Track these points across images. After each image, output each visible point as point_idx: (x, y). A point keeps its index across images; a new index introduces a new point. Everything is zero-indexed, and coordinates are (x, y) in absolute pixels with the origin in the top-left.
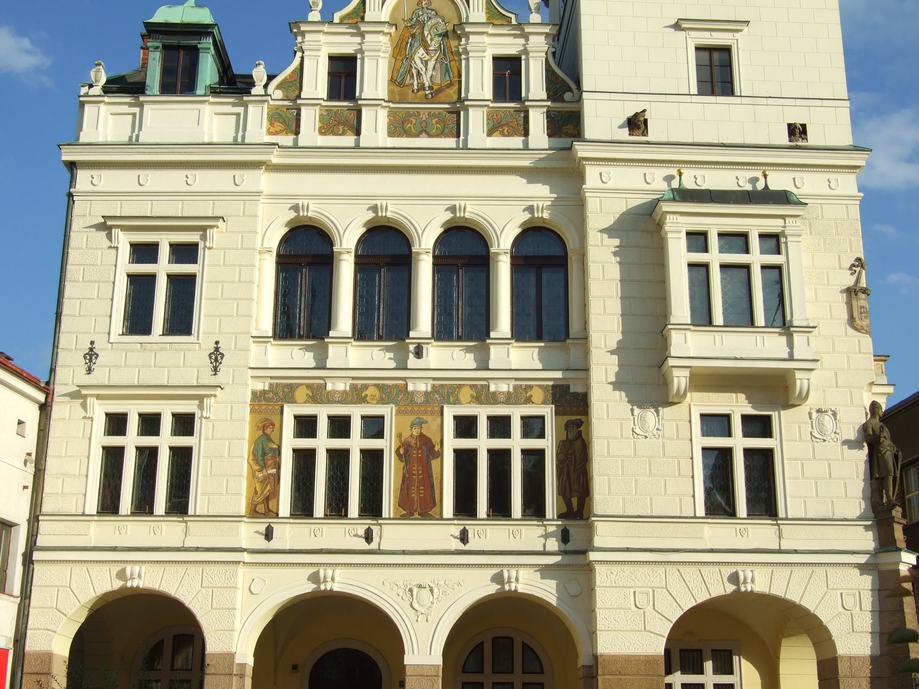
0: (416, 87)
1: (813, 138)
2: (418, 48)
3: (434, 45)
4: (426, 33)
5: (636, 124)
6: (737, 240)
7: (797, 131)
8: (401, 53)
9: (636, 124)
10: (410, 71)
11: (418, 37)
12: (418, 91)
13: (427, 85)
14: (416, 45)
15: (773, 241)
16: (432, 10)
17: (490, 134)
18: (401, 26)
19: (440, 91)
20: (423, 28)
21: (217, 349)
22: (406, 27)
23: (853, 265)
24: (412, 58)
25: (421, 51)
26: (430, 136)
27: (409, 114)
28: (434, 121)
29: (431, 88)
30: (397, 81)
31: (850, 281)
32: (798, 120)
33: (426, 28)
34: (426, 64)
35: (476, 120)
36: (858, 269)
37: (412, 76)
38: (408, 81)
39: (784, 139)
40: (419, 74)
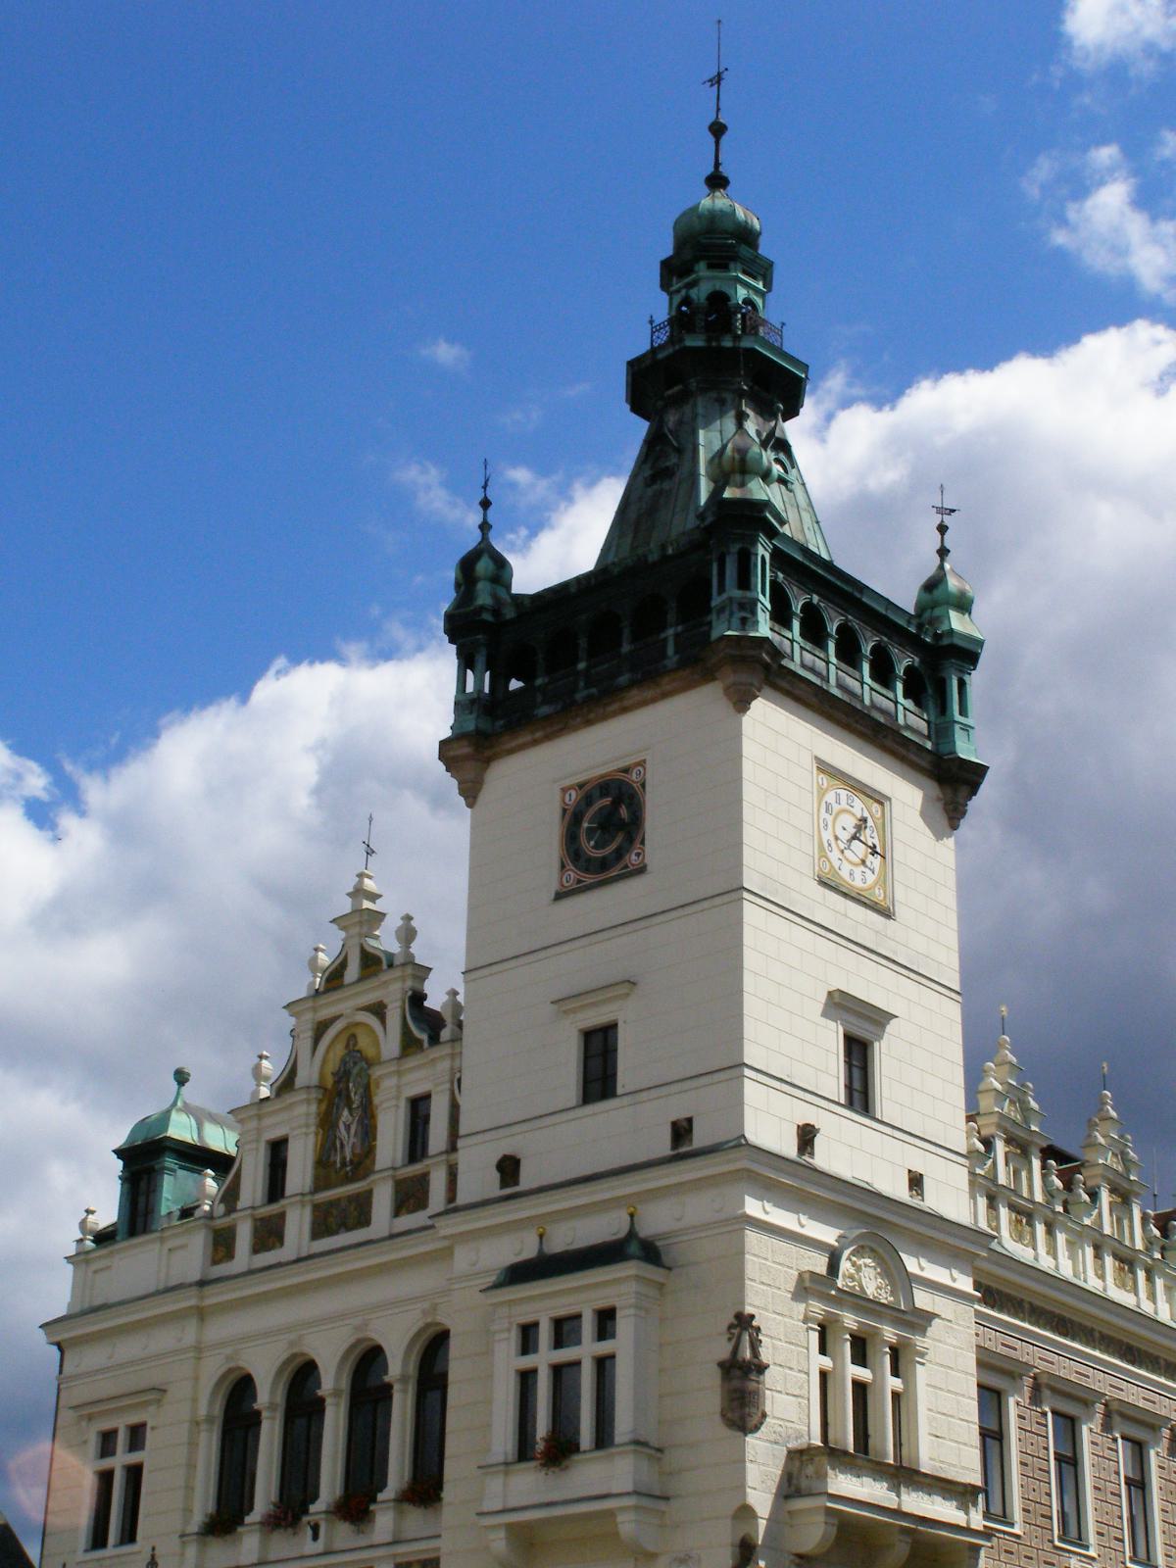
0: (338, 1165)
1: (700, 1138)
2: (343, 1109)
3: (356, 1099)
4: (351, 1085)
5: (509, 1168)
6: (565, 1330)
7: (681, 1131)
8: (327, 1123)
9: (509, 1168)
10: (334, 1145)
11: (344, 1093)
12: (341, 1168)
13: (348, 1159)
14: (342, 1104)
15: (606, 1319)
16: (358, 1051)
17: (397, 1213)
18: (330, 1082)
19: (360, 1163)
20: (348, 1081)
21: (153, 1556)
22: (335, 1082)
23: (731, 1327)
24: (338, 1127)
25: (346, 1113)
26: (349, 1229)
27: (333, 1204)
28: (352, 1208)
29: (351, 1161)
30: (322, 1163)
31: (723, 1351)
32: (679, 1114)
33: (351, 1080)
34: (348, 1128)
35: (383, 1198)
36: (736, 1331)
37: (336, 1150)
38: (332, 1159)
39: (663, 1146)
40: (342, 1145)
